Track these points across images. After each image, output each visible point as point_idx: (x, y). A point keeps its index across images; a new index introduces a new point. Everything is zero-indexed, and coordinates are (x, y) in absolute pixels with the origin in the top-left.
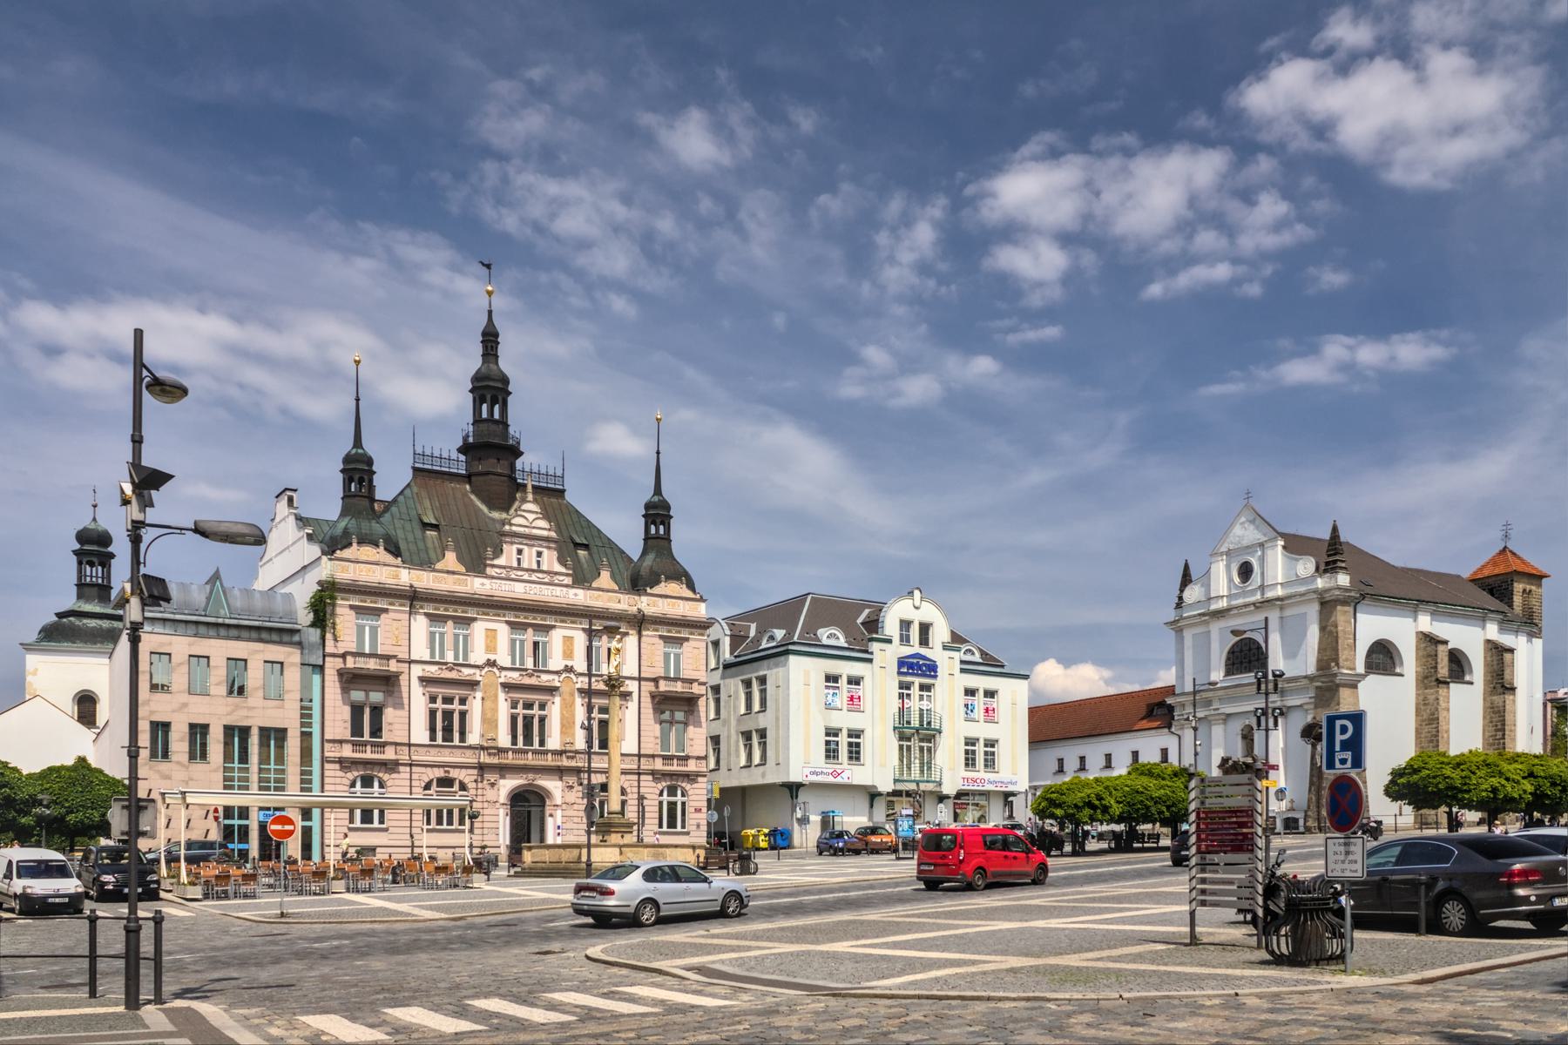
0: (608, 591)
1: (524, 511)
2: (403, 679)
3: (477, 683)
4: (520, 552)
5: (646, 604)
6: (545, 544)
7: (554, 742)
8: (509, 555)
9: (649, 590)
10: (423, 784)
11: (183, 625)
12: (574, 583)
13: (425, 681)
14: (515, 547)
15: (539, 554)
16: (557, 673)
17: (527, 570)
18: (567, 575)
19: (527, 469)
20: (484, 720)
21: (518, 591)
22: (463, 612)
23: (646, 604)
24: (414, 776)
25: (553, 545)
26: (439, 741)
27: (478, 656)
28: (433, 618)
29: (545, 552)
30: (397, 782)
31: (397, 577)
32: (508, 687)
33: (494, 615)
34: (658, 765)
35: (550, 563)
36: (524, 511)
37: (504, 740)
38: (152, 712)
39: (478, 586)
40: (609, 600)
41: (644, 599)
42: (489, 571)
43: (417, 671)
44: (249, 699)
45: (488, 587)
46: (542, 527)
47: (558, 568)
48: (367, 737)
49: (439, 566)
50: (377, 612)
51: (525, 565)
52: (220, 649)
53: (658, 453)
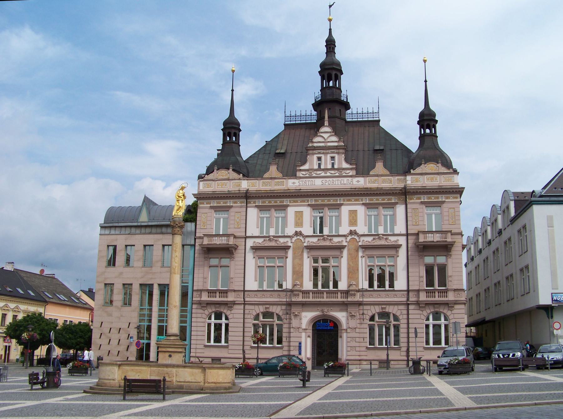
0: (382, 176)
1: (322, 132)
2: (241, 248)
4: (319, 159)
6: (335, 151)
7: (343, 285)
8: (313, 161)
9: (412, 171)
10: (252, 317)
11: (114, 228)
12: (357, 174)
13: (255, 249)
14: (315, 157)
15: (333, 158)
17: (323, 170)
18: (351, 169)
19: (355, 112)
20: (294, 272)
21: (318, 184)
22: (280, 202)
24: (246, 312)
25: (341, 151)
26: (376, 287)
27: (290, 230)
28: (261, 208)
29: (336, 156)
30: (235, 316)
32: (310, 248)
33: (301, 202)
34: (205, 297)
35: (340, 163)
36: (322, 132)
37: (308, 285)
38: (106, 278)
39: (292, 184)
40: (384, 182)
41: (409, 178)
42: (299, 174)
43: (250, 243)
44: (153, 268)
45: (297, 184)
46: (333, 140)
47: (345, 165)
48: (437, 287)
50: (226, 209)
51: (322, 167)
53: (426, 81)
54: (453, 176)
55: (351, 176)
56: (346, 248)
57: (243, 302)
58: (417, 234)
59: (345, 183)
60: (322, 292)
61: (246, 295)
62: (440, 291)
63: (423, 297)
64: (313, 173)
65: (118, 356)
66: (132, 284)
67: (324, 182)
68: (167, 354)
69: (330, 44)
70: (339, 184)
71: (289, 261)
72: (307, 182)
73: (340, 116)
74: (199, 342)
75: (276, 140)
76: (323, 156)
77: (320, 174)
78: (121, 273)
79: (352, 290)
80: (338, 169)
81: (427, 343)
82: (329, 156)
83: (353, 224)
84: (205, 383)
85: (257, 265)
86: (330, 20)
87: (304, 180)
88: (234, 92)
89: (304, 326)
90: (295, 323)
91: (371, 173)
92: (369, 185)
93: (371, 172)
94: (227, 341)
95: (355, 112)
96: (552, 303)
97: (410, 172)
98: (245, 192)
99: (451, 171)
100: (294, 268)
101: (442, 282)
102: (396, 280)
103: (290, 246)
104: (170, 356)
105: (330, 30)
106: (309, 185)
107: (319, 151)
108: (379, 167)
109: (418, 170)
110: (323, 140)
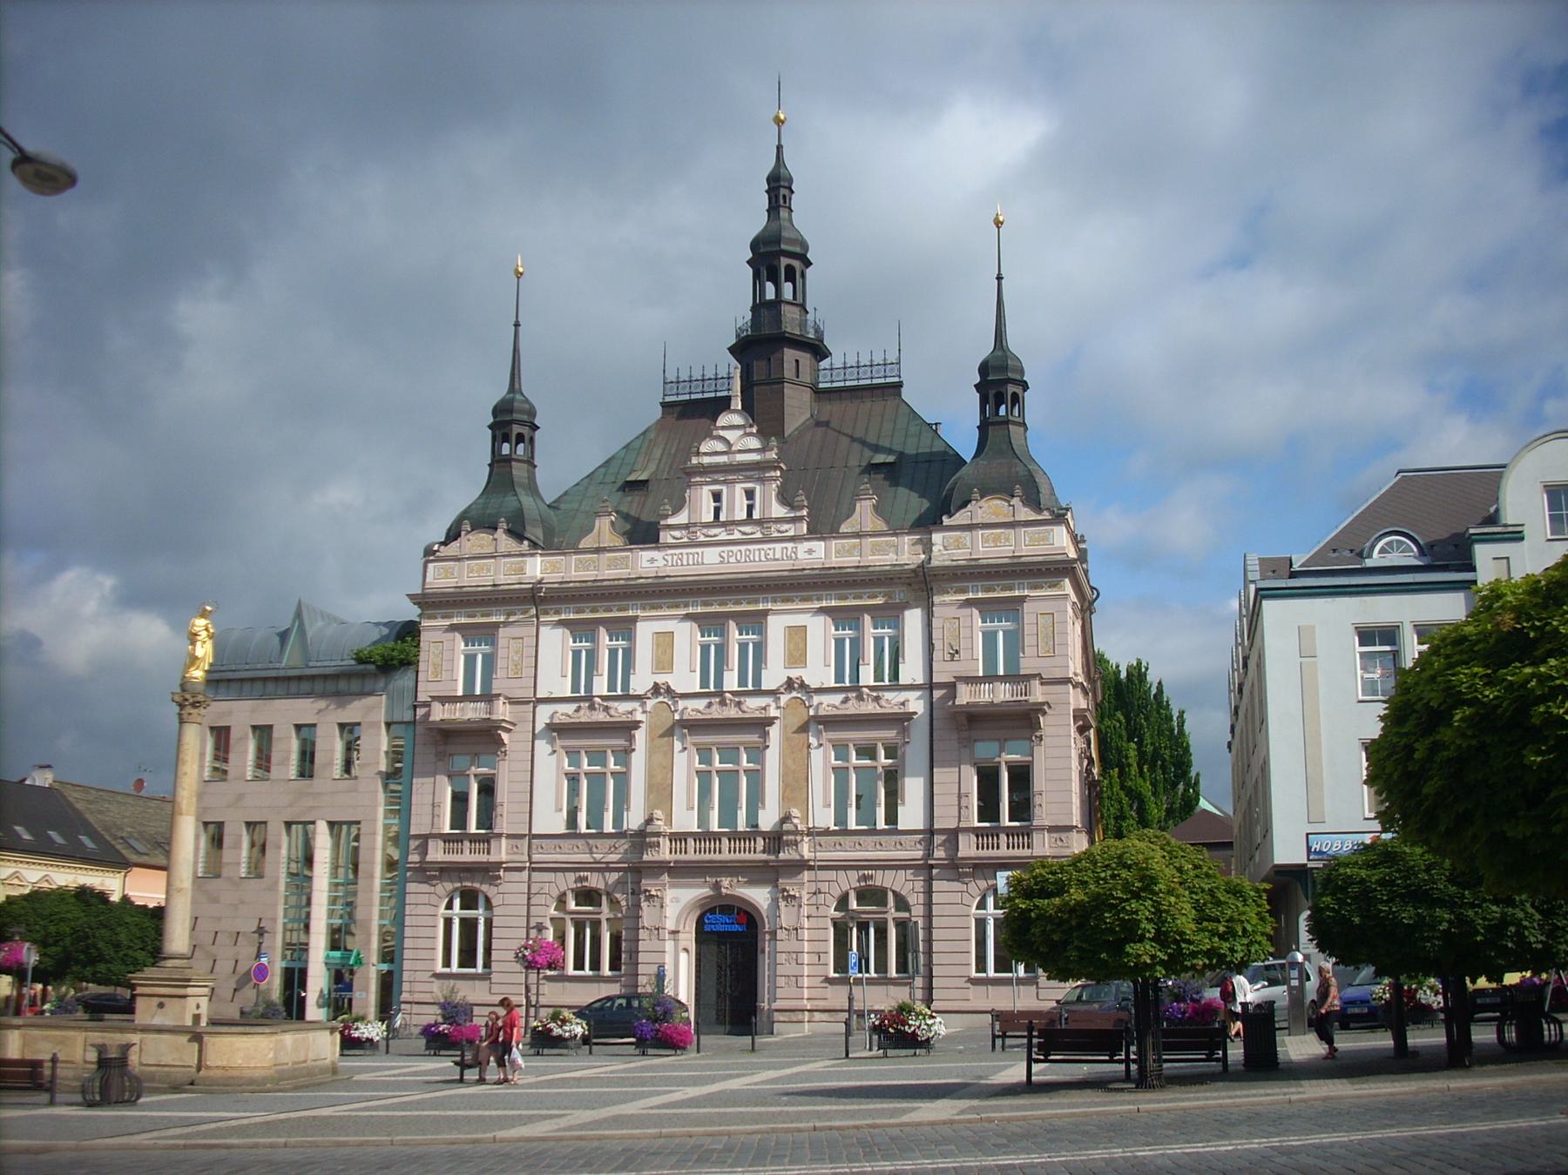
1: (723, 428)
3: (770, 721)
5: (946, 548)
6: (756, 474)
9: (946, 521)
13: (558, 730)
16: (773, 693)
17: (724, 525)
19: (838, 363)
21: (711, 561)
23: (946, 548)
30: (510, 899)
31: (521, 571)
36: (723, 428)
39: (648, 563)
40: (876, 550)
42: (666, 537)
43: (544, 714)
45: (661, 563)
47: (778, 511)
49: (585, 543)
52: (284, 713)
53: (999, 278)
54: (1052, 530)
55: (792, 539)
56: (777, 722)
57: (528, 864)
58: (951, 687)
59: (776, 557)
60: (716, 837)
61: (534, 847)
62: (1010, 832)
63: (968, 848)
64: (698, 533)
65: (232, 1001)
66: (265, 823)
67: (725, 555)
68: (156, 1001)
69: (779, 187)
70: (763, 559)
71: (638, 760)
72: (685, 556)
73: (798, 377)
74: (419, 965)
75: (637, 444)
76: (724, 488)
77: (715, 536)
78: (241, 797)
79: (789, 833)
80: (760, 522)
81: (981, 965)
82: (739, 489)
83: (796, 662)
84: (199, 1069)
85: (564, 772)
86: (779, 122)
87: (677, 551)
88: (520, 328)
89: (670, 925)
90: (647, 914)
91: (844, 528)
92: (835, 561)
93: (843, 526)
94: (487, 965)
95: (838, 363)
96: (1309, 860)
97: (942, 522)
98: (531, 586)
99: (1046, 515)
100: (650, 775)
101: (1022, 809)
102: (903, 804)
103: (640, 722)
104: (161, 1005)
105: (779, 148)
106: (688, 564)
107: (716, 477)
108: (864, 514)
109: (961, 517)
110: (720, 447)
